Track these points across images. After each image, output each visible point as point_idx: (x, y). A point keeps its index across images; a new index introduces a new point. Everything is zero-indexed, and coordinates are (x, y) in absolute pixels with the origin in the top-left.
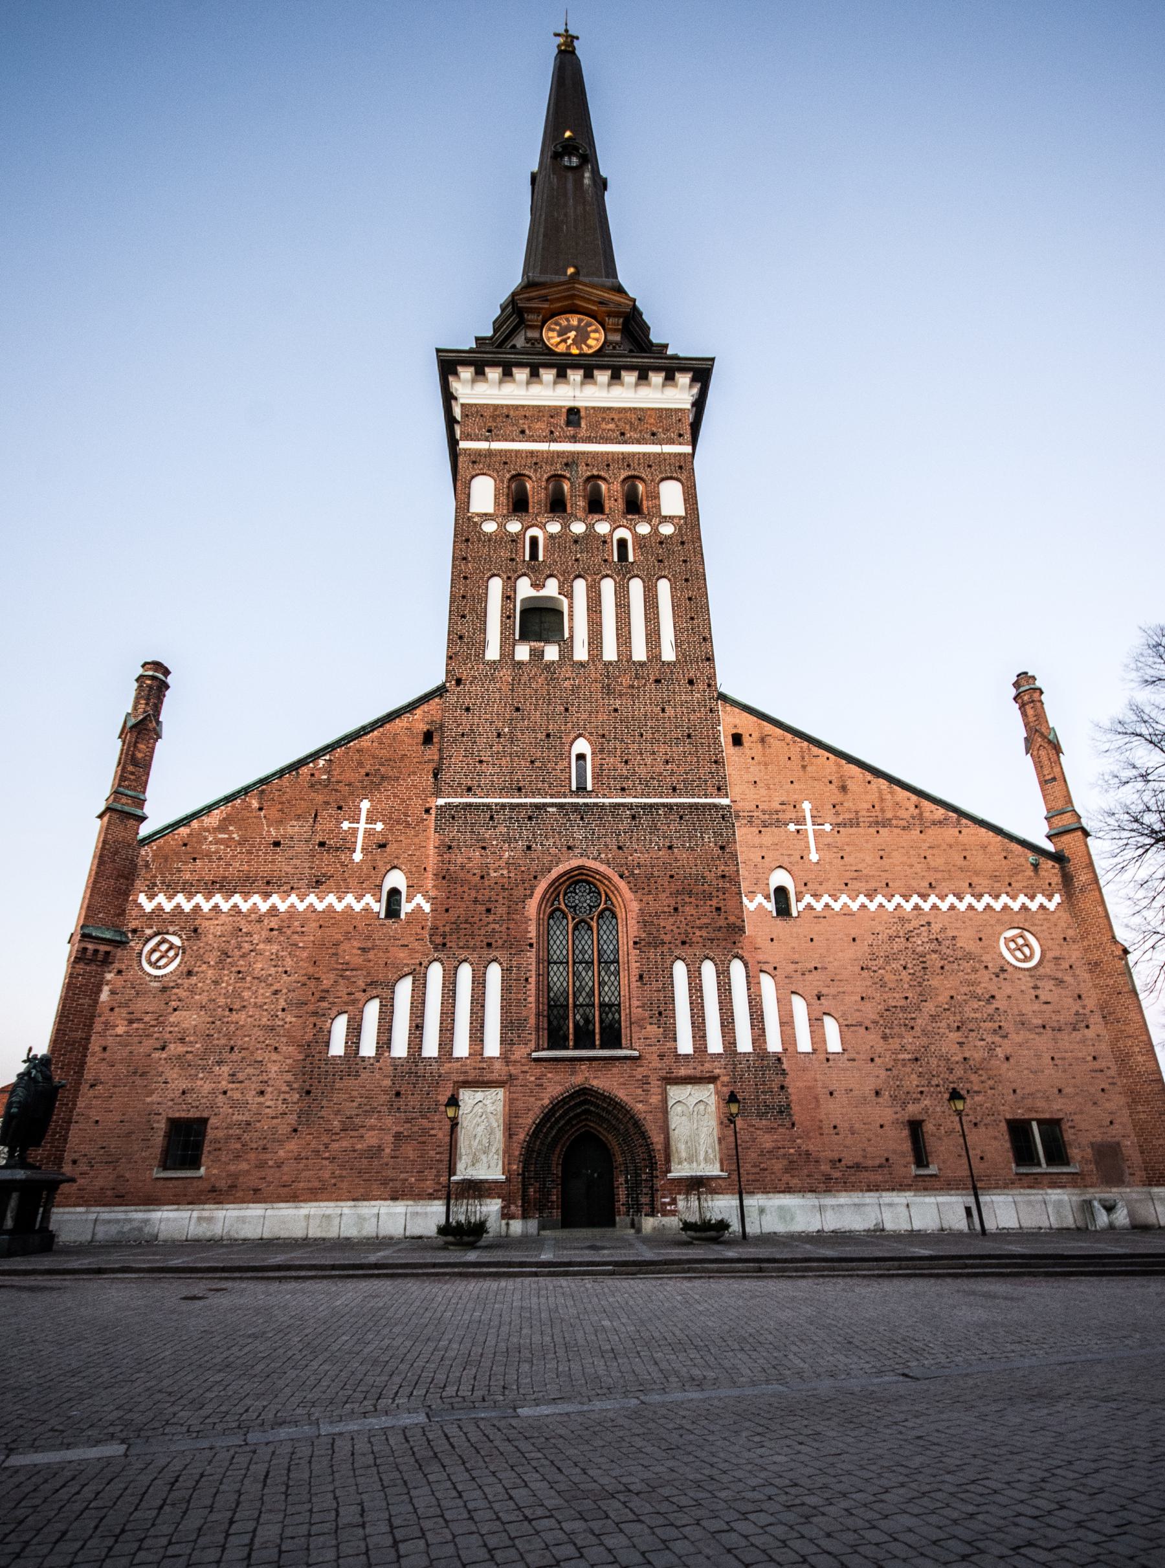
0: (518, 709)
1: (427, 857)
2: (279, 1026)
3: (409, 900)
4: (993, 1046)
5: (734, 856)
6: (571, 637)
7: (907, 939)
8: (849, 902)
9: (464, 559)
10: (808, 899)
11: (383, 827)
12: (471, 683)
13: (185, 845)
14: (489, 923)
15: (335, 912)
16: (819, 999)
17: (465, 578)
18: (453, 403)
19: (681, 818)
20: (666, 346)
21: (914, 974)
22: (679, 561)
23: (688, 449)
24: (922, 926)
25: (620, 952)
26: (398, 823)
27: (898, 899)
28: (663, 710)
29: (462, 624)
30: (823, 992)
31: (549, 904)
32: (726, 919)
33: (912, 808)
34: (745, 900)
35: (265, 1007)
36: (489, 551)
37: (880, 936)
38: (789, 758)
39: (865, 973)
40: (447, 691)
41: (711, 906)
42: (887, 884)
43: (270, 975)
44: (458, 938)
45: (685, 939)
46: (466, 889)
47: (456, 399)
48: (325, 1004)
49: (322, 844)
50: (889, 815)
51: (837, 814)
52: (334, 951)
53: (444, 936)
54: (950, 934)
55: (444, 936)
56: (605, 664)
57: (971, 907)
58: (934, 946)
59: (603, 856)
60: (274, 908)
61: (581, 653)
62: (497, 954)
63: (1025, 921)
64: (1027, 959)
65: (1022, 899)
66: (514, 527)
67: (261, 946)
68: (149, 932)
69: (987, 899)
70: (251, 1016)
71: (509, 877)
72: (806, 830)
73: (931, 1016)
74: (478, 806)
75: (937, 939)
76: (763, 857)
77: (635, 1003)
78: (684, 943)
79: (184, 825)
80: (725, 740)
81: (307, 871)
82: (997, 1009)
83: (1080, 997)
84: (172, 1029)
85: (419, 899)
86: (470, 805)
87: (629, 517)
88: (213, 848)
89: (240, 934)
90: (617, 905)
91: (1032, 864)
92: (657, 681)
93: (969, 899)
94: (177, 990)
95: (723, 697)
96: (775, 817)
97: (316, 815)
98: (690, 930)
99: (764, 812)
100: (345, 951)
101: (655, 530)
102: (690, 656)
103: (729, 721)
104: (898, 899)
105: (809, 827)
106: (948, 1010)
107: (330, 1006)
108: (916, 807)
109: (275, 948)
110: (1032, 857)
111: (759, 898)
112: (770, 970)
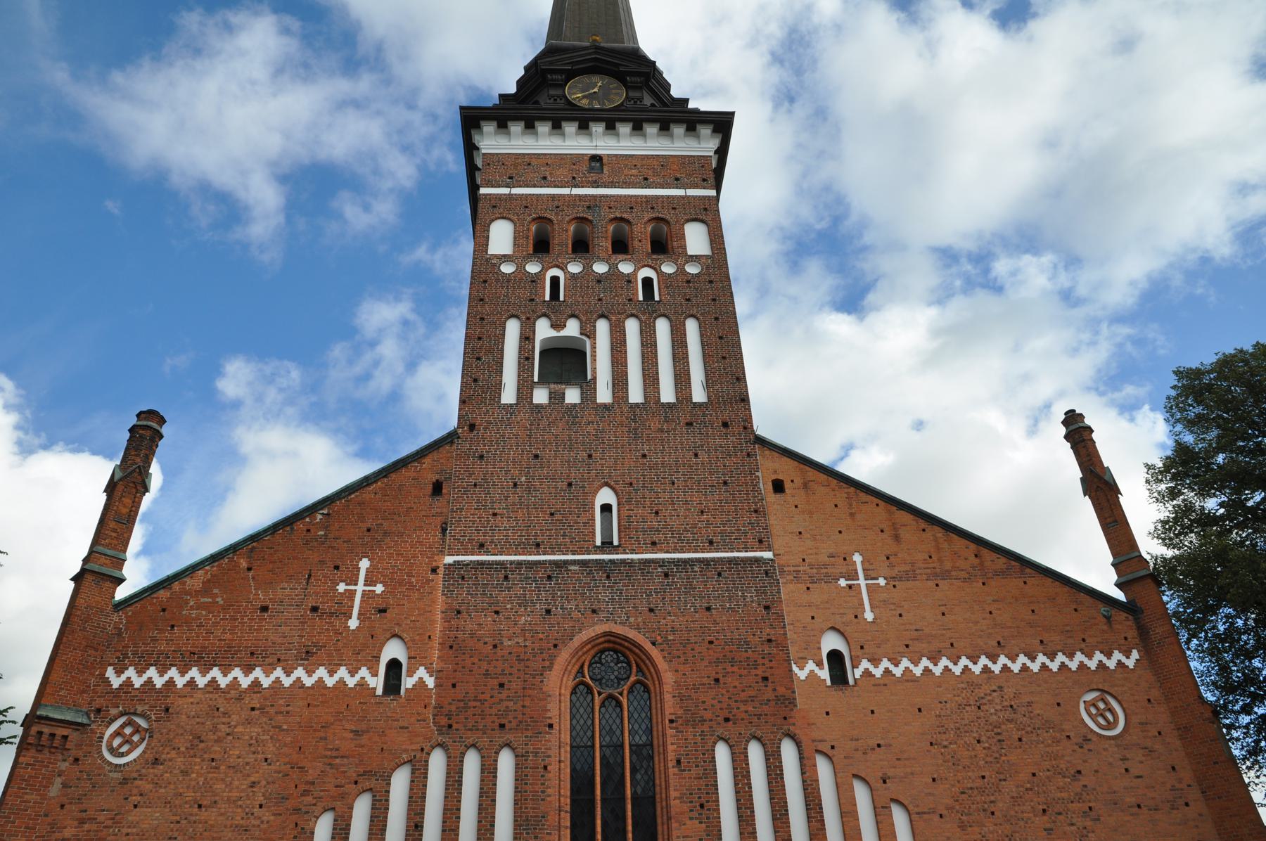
0: (536, 456)
1: (433, 622)
2: (254, 826)
3: (410, 674)
4: (1085, 831)
5: (780, 617)
6: (594, 379)
7: (979, 708)
8: (912, 667)
9: (482, 300)
10: (865, 664)
11: (383, 589)
12: (485, 429)
13: (164, 610)
14: (502, 700)
15: (325, 687)
16: (885, 782)
17: (482, 319)
18: (475, 153)
19: (719, 574)
20: (687, 101)
21: (989, 748)
22: (708, 300)
23: (713, 193)
24: (994, 691)
25: (655, 733)
26: (401, 583)
27: (964, 661)
28: (696, 455)
29: (476, 366)
30: (889, 774)
31: (572, 677)
32: (774, 690)
33: (972, 558)
34: (795, 668)
35: (240, 803)
36: (508, 293)
37: (948, 705)
38: (836, 506)
39: (934, 750)
40: (459, 438)
41: (756, 675)
42: (952, 645)
43: (247, 764)
44: (466, 718)
45: (727, 715)
46: (476, 661)
47: (478, 149)
48: (309, 799)
49: (314, 609)
50: (948, 566)
51: (892, 566)
52: (323, 735)
53: (449, 716)
54: (1026, 699)
55: (449, 716)
56: (631, 407)
57: (1044, 667)
58: (1008, 714)
59: (632, 620)
60: (256, 683)
61: (604, 395)
62: (509, 737)
63: (1103, 681)
64: (1111, 726)
65: (1098, 656)
66: (533, 268)
67: (240, 729)
68: (114, 711)
69: (1061, 658)
70: (222, 814)
71: (525, 646)
72: (859, 584)
73: (1013, 797)
74: (490, 564)
75: (1011, 706)
76: (813, 618)
77: (673, 794)
78: (727, 720)
79: (164, 588)
80: (765, 487)
81: (296, 640)
82: (1085, 786)
83: (1173, 768)
84: (129, 830)
85: (422, 672)
86: (482, 563)
87: (654, 257)
88: (194, 613)
89: (217, 714)
90: (649, 676)
91: (1105, 616)
92: (689, 424)
93: (1041, 658)
94: (140, 782)
95: (762, 442)
96: (824, 571)
97: (310, 576)
98: (733, 705)
99: (811, 566)
100: (334, 734)
101: (681, 270)
102: (723, 397)
103: (768, 468)
104: (964, 661)
105: (862, 582)
106: (1031, 789)
107: (314, 801)
108: (976, 556)
109: (255, 730)
110: (1103, 609)
111: (811, 666)
112: (826, 748)
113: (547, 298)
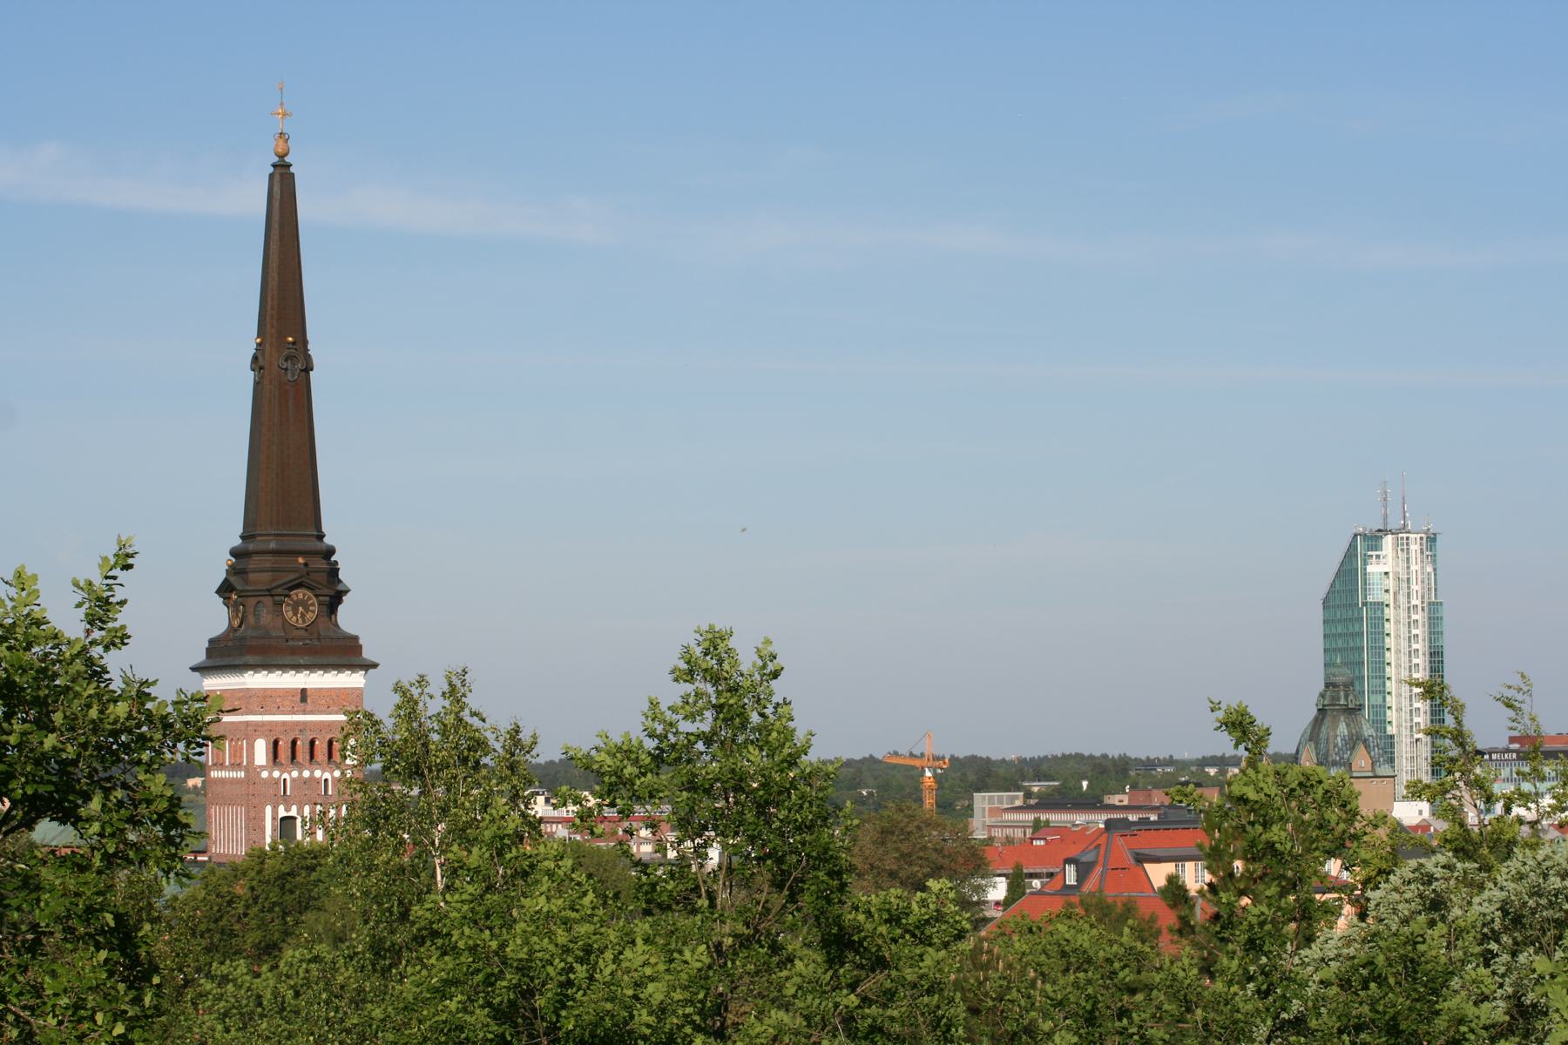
66: (276, 774)
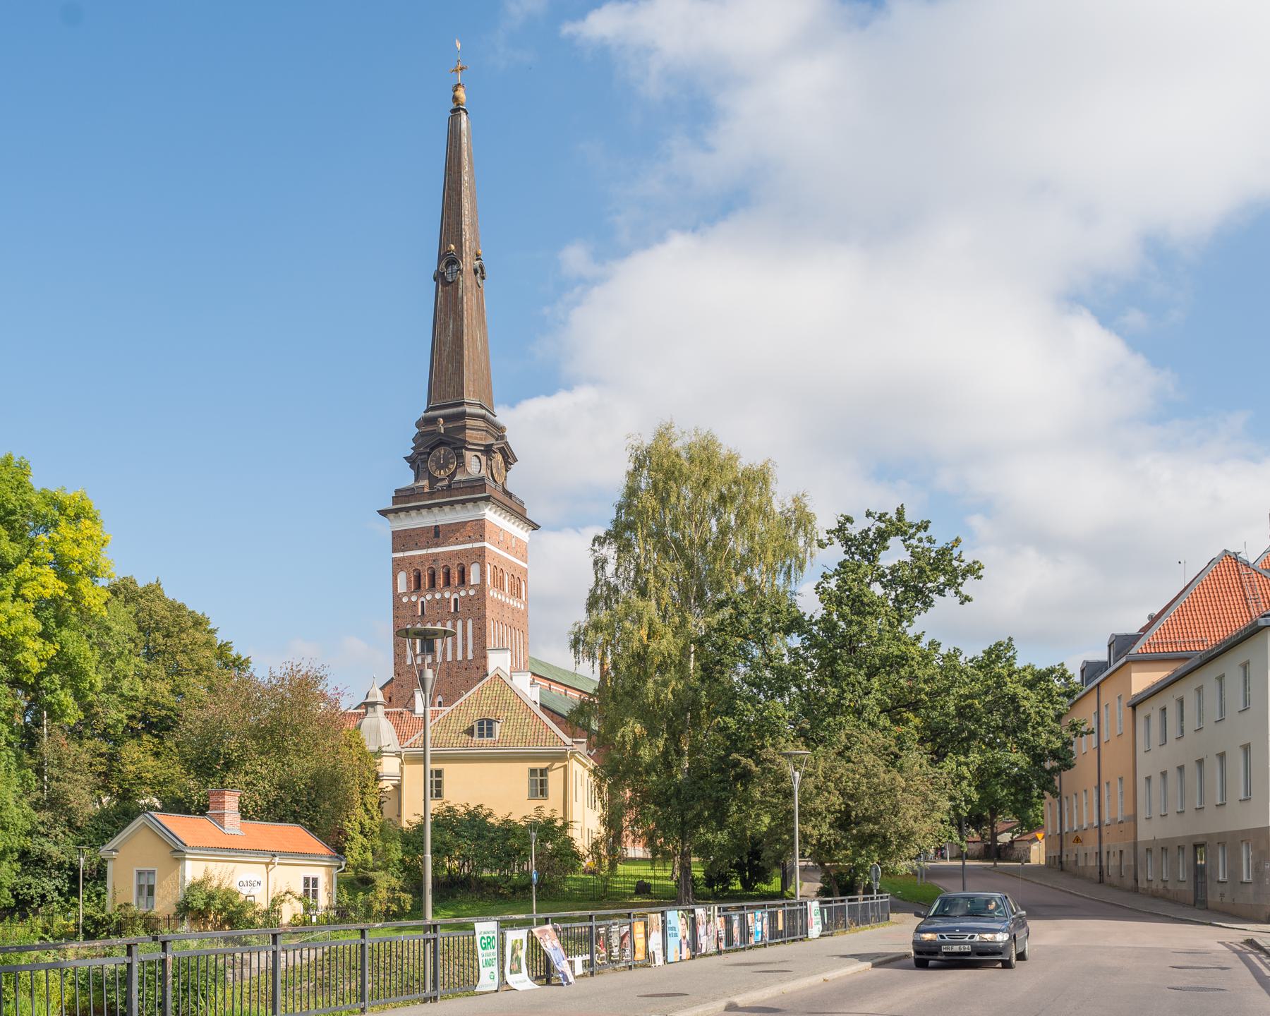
66: (414, 599)
113: (420, 614)
